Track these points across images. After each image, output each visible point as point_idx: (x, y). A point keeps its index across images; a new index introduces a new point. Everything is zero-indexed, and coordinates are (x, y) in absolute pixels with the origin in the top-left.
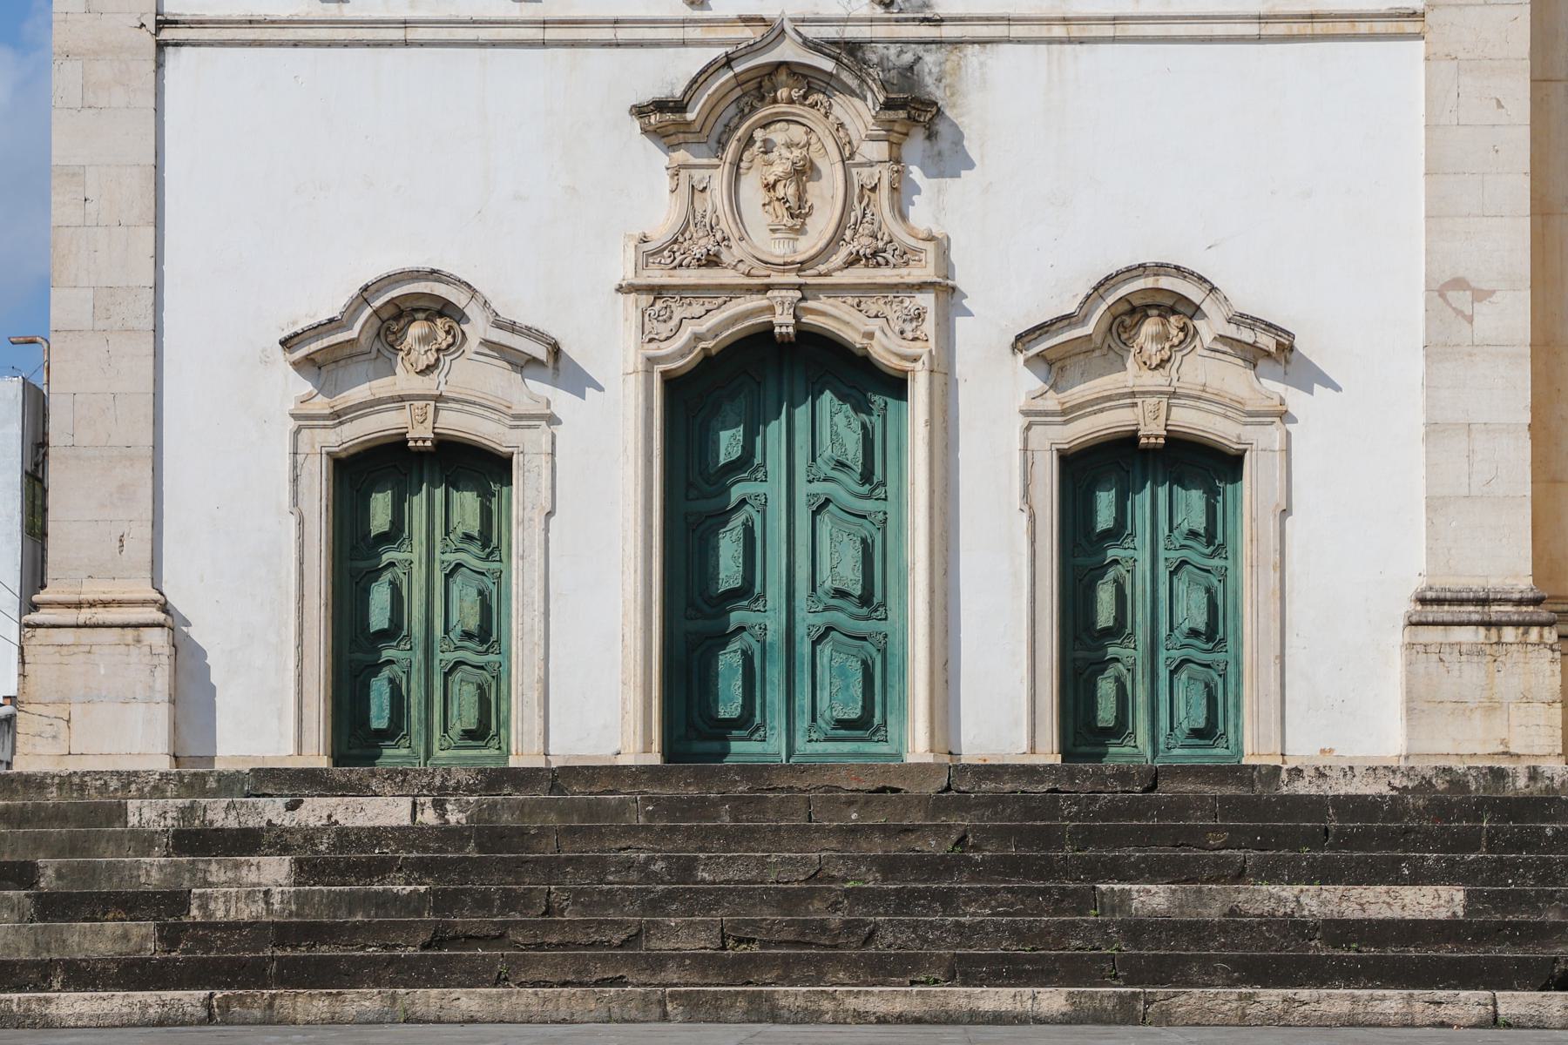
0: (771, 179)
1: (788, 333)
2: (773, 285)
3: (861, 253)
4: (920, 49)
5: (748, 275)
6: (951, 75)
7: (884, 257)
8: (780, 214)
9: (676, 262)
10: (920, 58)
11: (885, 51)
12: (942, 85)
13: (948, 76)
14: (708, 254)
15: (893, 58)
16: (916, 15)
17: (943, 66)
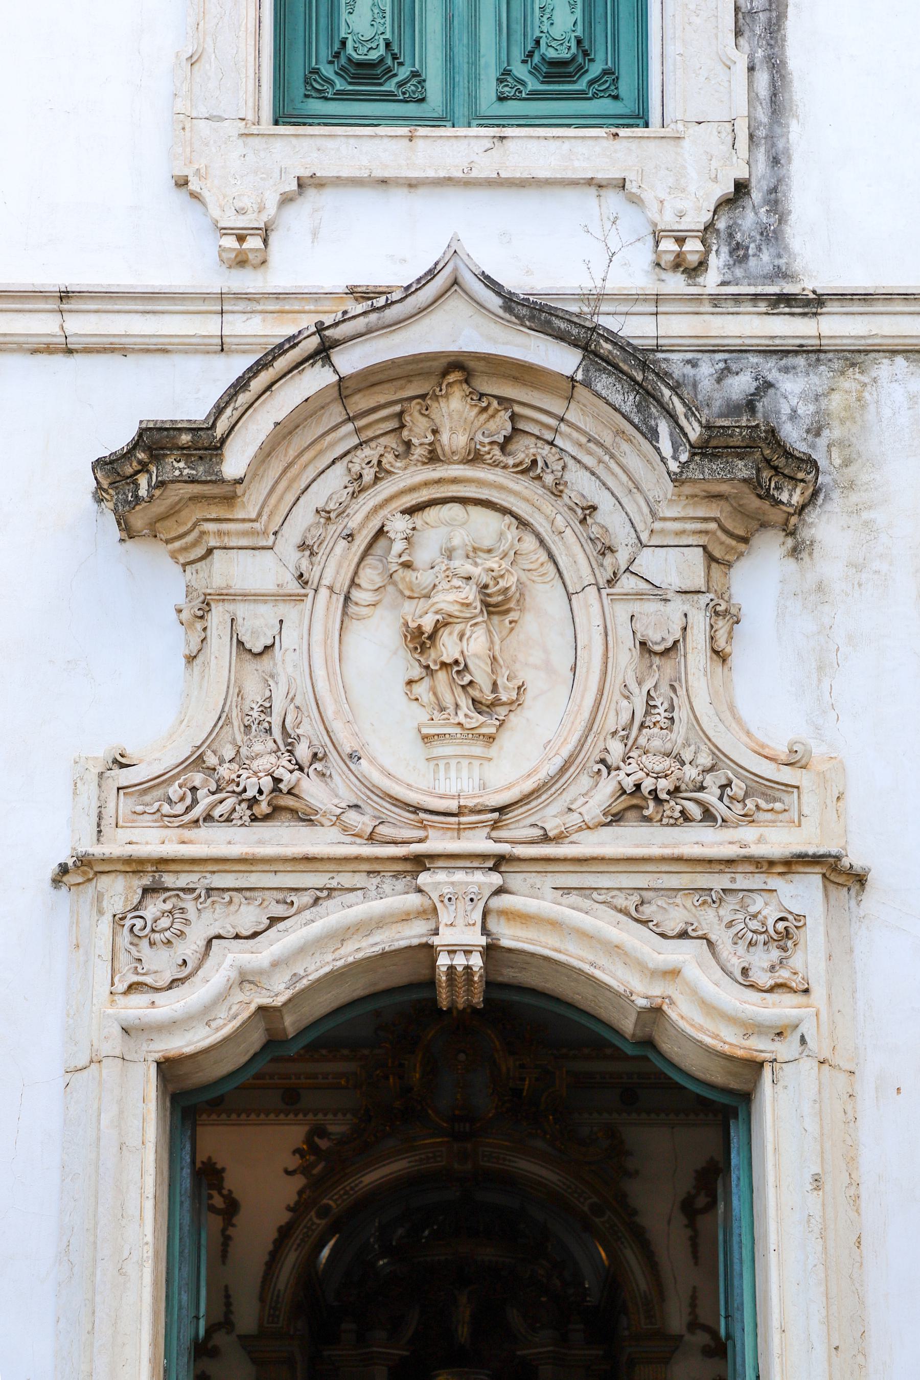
0: (428, 624)
1: (468, 968)
2: (432, 857)
3: (648, 784)
4: (770, 369)
5: (371, 838)
6: (842, 422)
7: (696, 801)
8: (448, 700)
9: (197, 812)
10: (769, 385)
11: (688, 370)
12: (822, 442)
13: (835, 423)
14: (276, 789)
15: (706, 385)
16: (759, 290)
17: (824, 402)
